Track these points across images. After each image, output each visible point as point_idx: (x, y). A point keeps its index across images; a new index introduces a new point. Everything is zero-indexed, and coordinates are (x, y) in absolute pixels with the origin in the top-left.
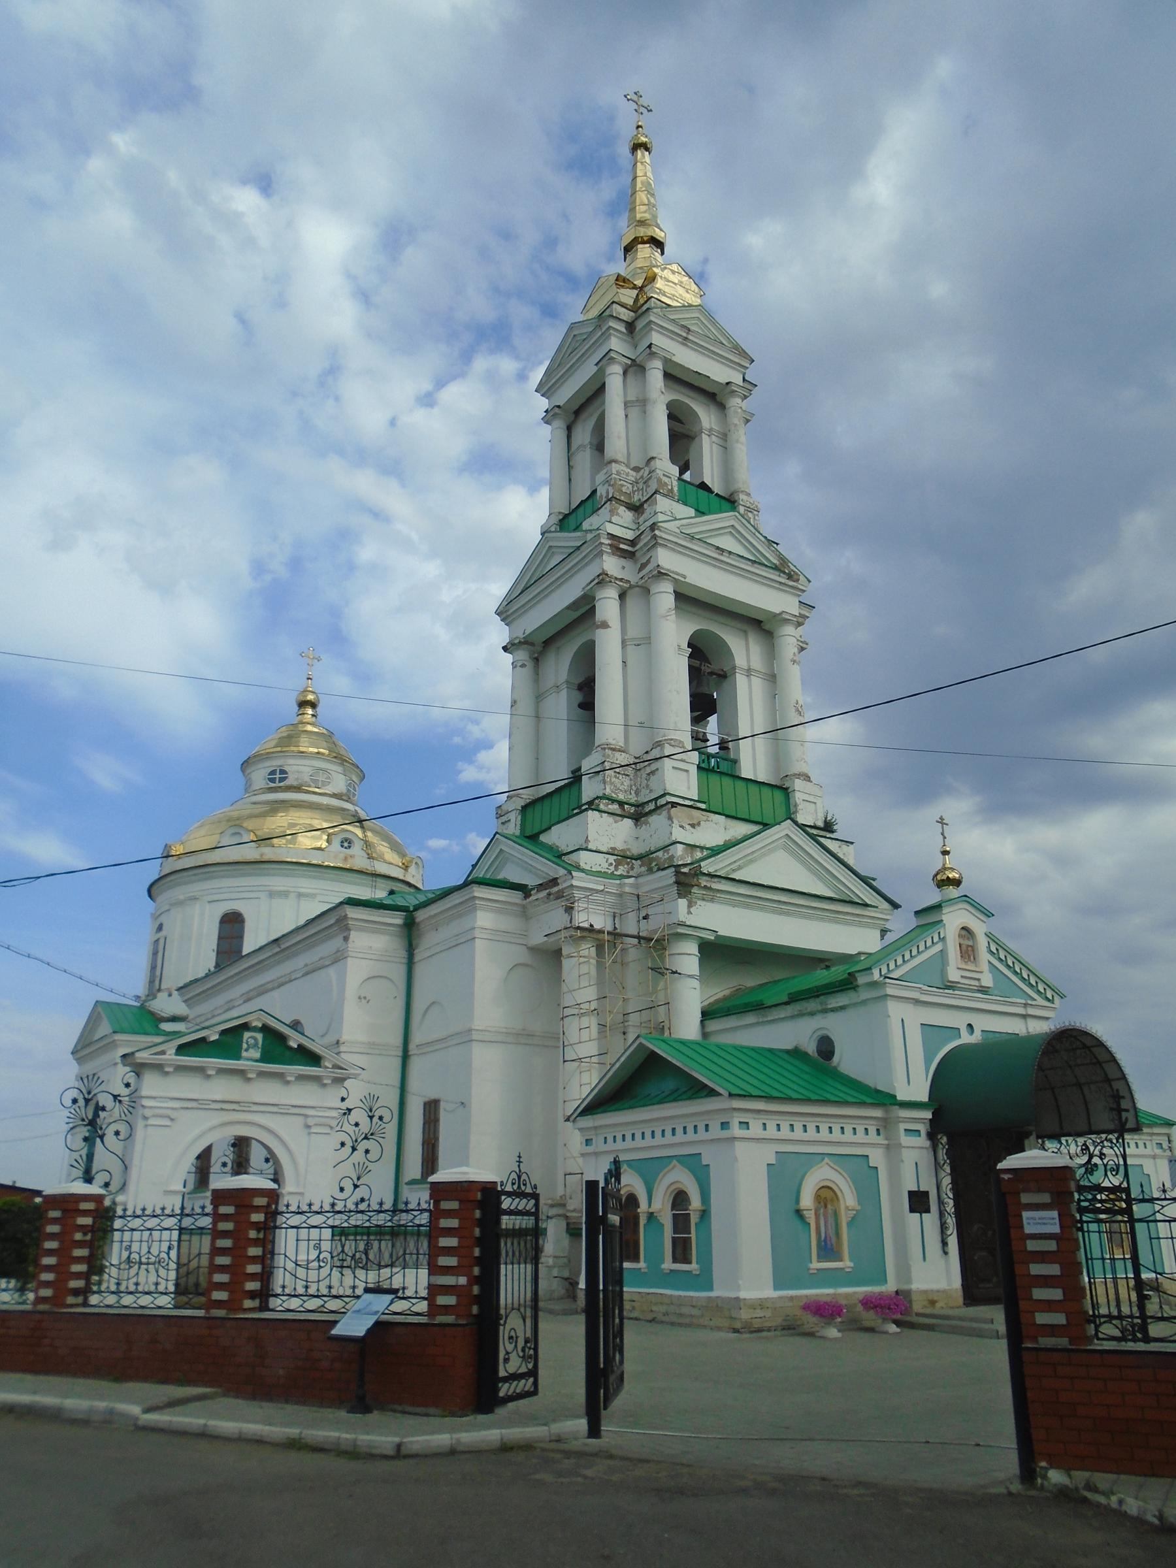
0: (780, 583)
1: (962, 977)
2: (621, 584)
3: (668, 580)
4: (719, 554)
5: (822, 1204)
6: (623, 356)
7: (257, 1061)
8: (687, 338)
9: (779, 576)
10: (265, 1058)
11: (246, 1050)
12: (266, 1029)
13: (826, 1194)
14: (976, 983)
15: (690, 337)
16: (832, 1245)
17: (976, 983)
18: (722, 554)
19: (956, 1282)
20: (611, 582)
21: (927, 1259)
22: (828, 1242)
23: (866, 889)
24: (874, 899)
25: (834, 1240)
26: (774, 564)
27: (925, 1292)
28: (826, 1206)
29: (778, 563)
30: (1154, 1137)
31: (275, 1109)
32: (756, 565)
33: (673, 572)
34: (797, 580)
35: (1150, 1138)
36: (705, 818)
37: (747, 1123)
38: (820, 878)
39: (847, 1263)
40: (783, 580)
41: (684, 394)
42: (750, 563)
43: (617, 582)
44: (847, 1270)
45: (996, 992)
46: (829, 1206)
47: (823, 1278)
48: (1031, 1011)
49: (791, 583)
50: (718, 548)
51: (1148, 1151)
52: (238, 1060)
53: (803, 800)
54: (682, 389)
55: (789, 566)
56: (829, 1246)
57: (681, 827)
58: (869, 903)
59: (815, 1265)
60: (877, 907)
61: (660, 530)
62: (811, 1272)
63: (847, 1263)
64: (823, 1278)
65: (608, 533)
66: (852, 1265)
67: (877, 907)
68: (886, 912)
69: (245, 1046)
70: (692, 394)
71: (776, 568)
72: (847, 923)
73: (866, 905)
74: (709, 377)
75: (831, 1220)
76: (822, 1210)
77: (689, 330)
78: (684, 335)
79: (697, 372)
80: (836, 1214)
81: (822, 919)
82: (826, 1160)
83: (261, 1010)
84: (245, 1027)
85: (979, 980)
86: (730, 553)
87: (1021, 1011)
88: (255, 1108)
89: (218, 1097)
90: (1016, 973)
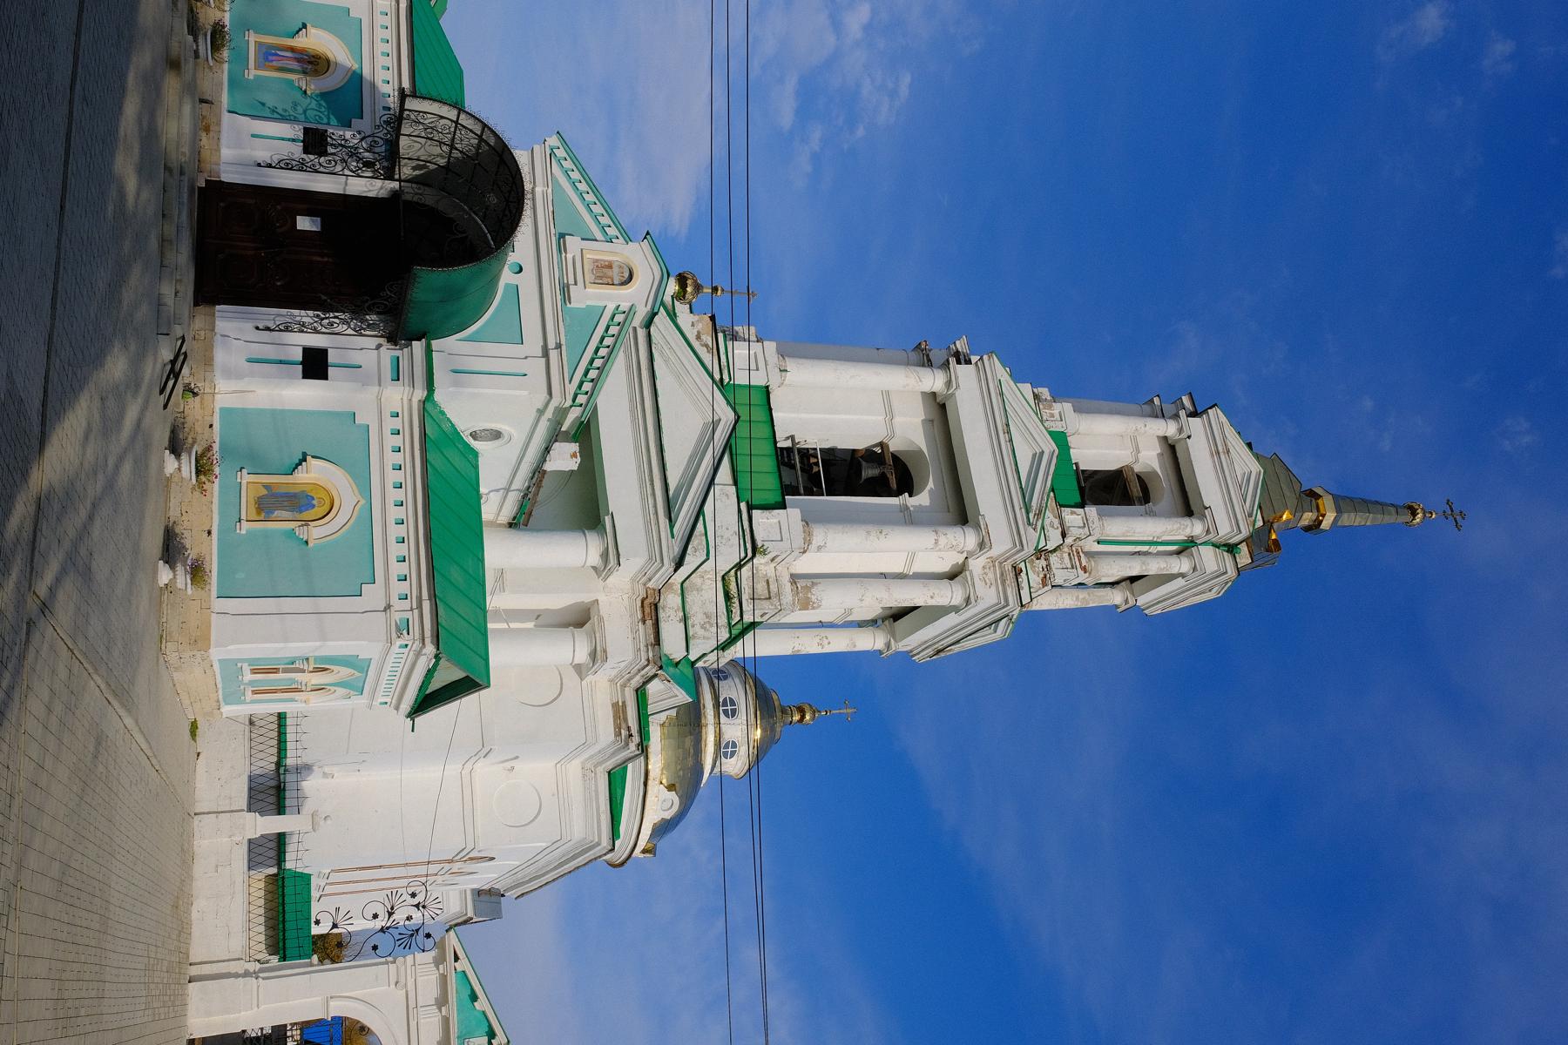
14: (571, 281)
17: (571, 281)
20: (922, 351)
22: (274, 58)
25: (275, 63)
27: (219, 124)
30: (416, 612)
35: (414, 606)
37: (398, 380)
48: (553, 354)
50: (1008, 425)
51: (397, 604)
56: (270, 58)
57: (693, 325)
60: (673, 537)
61: (989, 359)
66: (251, 77)
67: (673, 537)
68: (671, 551)
72: (643, 499)
73: (672, 527)
77: (1228, 452)
85: (576, 284)
86: (1011, 440)
87: (551, 344)
90: (596, 351)
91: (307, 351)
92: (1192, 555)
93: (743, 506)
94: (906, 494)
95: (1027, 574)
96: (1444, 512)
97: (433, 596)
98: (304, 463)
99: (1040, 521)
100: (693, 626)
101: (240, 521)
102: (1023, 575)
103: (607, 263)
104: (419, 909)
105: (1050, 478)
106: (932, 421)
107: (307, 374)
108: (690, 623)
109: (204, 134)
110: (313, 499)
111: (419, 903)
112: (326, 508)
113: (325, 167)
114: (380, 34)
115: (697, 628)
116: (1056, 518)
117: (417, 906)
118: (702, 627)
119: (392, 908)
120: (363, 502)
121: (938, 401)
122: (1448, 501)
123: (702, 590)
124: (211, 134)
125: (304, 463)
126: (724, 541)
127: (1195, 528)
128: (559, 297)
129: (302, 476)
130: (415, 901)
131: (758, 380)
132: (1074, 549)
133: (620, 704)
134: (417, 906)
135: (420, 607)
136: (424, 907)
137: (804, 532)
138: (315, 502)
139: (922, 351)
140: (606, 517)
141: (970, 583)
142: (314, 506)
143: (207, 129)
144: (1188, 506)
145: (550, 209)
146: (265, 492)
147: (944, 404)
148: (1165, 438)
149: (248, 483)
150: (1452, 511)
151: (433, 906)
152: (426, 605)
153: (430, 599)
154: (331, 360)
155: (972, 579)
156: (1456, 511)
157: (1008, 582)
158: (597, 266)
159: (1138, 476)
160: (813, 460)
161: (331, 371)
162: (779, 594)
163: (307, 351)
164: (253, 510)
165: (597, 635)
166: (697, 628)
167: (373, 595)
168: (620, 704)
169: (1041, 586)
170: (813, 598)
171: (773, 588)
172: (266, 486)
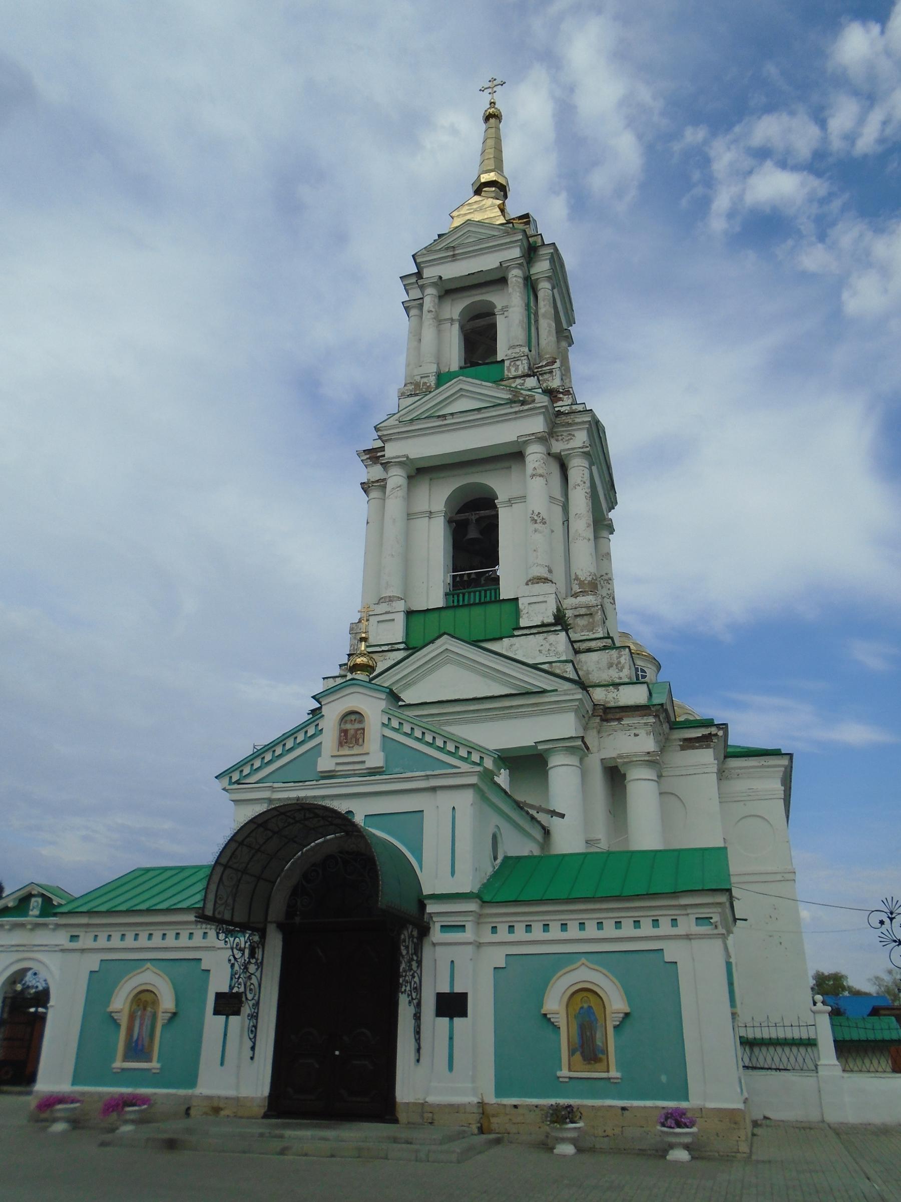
0: (516, 413)
1: (337, 764)
2: (379, 484)
3: (392, 465)
4: (443, 420)
5: (141, 1007)
6: (414, 300)
7: (37, 917)
8: (454, 255)
9: (511, 407)
10: (43, 914)
11: (32, 910)
12: (43, 896)
13: (144, 997)
15: (457, 252)
16: (143, 1045)
18: (446, 419)
19: (264, 1089)
20: (369, 487)
21: (226, 1063)
23: (541, 676)
24: (551, 683)
25: (146, 1043)
26: (507, 399)
27: (209, 1098)
28: (145, 1009)
29: (510, 396)
31: (46, 948)
32: (482, 411)
33: (394, 458)
34: (534, 401)
36: (382, 658)
38: (494, 679)
39: (155, 1065)
40: (517, 409)
41: (469, 296)
42: (477, 412)
43: (374, 485)
44: (154, 1071)
45: (396, 770)
46: (149, 1009)
47: (123, 1076)
49: (526, 407)
50: (439, 417)
51: (681, 930)
52: (26, 917)
53: (529, 604)
54: (468, 293)
55: (521, 394)
58: (549, 688)
59: (118, 1064)
62: (115, 1070)
63: (155, 1065)
64: (123, 1076)
65: (364, 451)
66: (158, 1065)
67: (556, 690)
69: (31, 907)
70: (484, 290)
71: (511, 402)
73: (544, 692)
74: (482, 271)
75: (147, 1022)
76: (139, 1013)
77: (453, 247)
78: (451, 253)
79: (469, 274)
80: (154, 1016)
81: (492, 719)
82: (149, 965)
83: (32, 883)
84: (30, 896)
85: (363, 762)
86: (452, 414)
88: (36, 948)
89: (13, 943)
91: (440, 1013)
92: (538, 279)
93: (516, 633)
94: (496, 501)
95: (562, 406)
96: (490, 93)
97: (675, 894)
98: (548, 1016)
99: (522, 391)
100: (620, 678)
101: (609, 1079)
102: (562, 409)
103: (343, 734)
104: (894, 918)
105: (484, 383)
106: (431, 480)
107: (462, 1012)
108: (618, 681)
109: (222, 1113)
110: (582, 1008)
111: (889, 917)
112: (589, 995)
113: (255, 995)
114: (116, 942)
115: (621, 674)
116: (515, 381)
117: (891, 919)
118: (621, 671)
119: (895, 941)
120: (583, 960)
121: (414, 474)
122: (480, 90)
123: (588, 670)
124: (221, 1105)
125: (548, 1016)
126: (553, 649)
127: (515, 276)
128: (378, 777)
129: (561, 1020)
130: (887, 921)
131: (400, 618)
132: (536, 370)
133: (681, 743)
134: (891, 919)
135: (685, 906)
136: (892, 913)
137: (538, 583)
138: (585, 1006)
139: (369, 487)
140: (539, 748)
141: (571, 452)
142: (590, 1007)
143: (217, 1110)
144: (498, 280)
145: (292, 784)
146: (578, 1053)
147: (417, 469)
148: (441, 297)
149: (570, 1070)
150: (489, 88)
151: (890, 904)
152: (684, 901)
153: (678, 897)
154: (446, 990)
155: (569, 449)
156: (490, 84)
157: (570, 421)
158: (346, 743)
159: (468, 321)
160: (465, 578)
161: (457, 990)
162: (588, 607)
163: (440, 1013)
164: (597, 1066)
165: (635, 759)
166: (621, 674)
167: (672, 951)
168: (681, 743)
169: (570, 396)
170: (589, 579)
171: (583, 611)
172: (572, 1052)
